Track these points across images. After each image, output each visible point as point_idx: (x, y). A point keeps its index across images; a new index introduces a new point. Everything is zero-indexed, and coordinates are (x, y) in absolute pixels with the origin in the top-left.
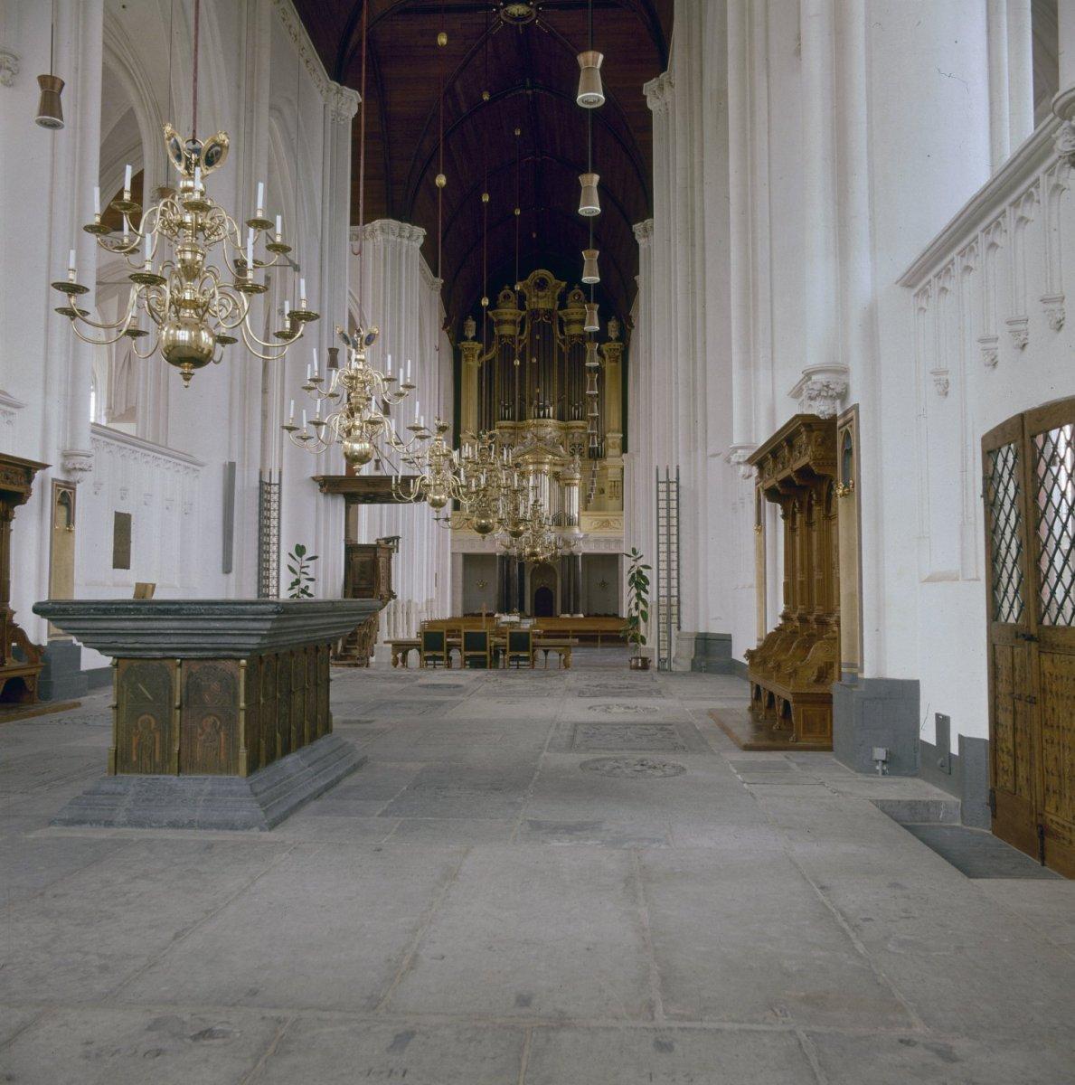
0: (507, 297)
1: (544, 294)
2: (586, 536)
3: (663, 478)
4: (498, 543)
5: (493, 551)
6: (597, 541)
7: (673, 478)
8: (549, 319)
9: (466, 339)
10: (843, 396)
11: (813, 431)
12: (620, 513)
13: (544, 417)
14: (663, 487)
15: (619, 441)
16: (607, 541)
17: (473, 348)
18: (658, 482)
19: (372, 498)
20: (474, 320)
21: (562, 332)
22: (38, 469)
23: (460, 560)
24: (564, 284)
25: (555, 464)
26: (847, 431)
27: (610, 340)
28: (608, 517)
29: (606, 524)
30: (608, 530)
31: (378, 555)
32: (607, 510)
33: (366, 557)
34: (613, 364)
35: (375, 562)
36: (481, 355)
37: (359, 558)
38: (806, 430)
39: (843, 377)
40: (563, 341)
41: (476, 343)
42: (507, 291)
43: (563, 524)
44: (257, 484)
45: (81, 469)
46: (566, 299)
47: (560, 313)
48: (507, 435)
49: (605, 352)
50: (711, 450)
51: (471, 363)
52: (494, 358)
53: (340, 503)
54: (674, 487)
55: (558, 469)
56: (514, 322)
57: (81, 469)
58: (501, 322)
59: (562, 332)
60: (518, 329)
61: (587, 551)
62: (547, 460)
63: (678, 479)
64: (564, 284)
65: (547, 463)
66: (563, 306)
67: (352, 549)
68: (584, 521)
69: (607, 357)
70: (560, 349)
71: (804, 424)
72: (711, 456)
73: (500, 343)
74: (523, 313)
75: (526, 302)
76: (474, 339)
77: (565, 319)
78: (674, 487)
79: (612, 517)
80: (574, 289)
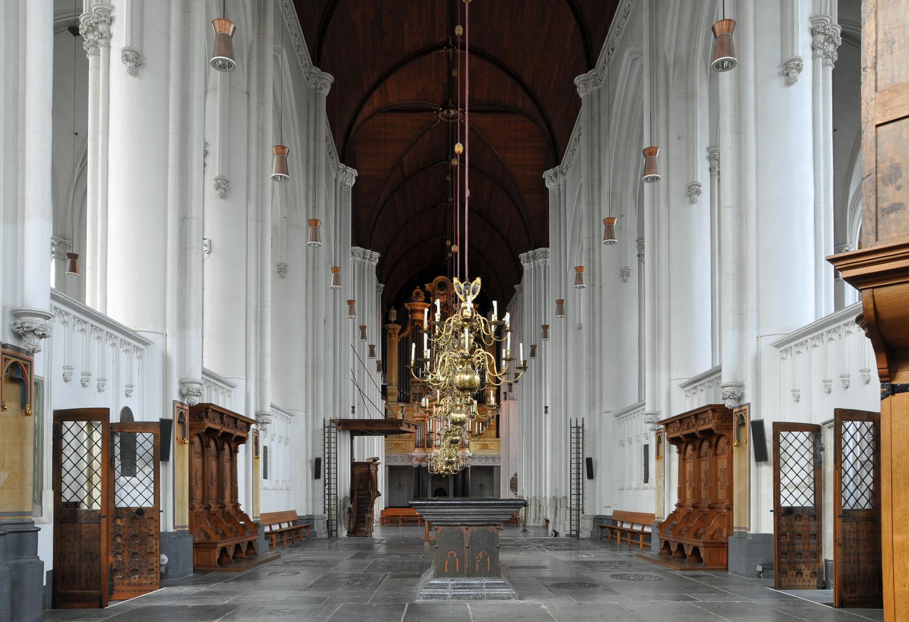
0: (418, 294)
2: (474, 455)
3: (574, 425)
5: (409, 464)
6: (480, 458)
7: (580, 424)
8: (447, 310)
9: (390, 322)
10: (739, 399)
11: (715, 412)
12: (498, 439)
14: (574, 430)
16: (487, 458)
17: (395, 329)
18: (571, 427)
19: (363, 433)
22: (252, 424)
23: (387, 468)
26: (741, 416)
28: (487, 442)
29: (485, 447)
30: (487, 450)
31: (371, 468)
32: (487, 438)
33: (364, 470)
35: (369, 472)
36: (399, 334)
37: (358, 471)
38: (712, 412)
39: (740, 389)
41: (397, 325)
42: (418, 290)
44: (323, 427)
45: (266, 423)
48: (419, 387)
50: (605, 409)
51: (393, 339)
52: (409, 335)
53: (348, 436)
54: (581, 430)
57: (266, 423)
61: (473, 464)
63: (583, 425)
67: (354, 465)
68: (472, 444)
71: (711, 409)
72: (604, 413)
76: (395, 322)
78: (581, 430)
79: (490, 442)
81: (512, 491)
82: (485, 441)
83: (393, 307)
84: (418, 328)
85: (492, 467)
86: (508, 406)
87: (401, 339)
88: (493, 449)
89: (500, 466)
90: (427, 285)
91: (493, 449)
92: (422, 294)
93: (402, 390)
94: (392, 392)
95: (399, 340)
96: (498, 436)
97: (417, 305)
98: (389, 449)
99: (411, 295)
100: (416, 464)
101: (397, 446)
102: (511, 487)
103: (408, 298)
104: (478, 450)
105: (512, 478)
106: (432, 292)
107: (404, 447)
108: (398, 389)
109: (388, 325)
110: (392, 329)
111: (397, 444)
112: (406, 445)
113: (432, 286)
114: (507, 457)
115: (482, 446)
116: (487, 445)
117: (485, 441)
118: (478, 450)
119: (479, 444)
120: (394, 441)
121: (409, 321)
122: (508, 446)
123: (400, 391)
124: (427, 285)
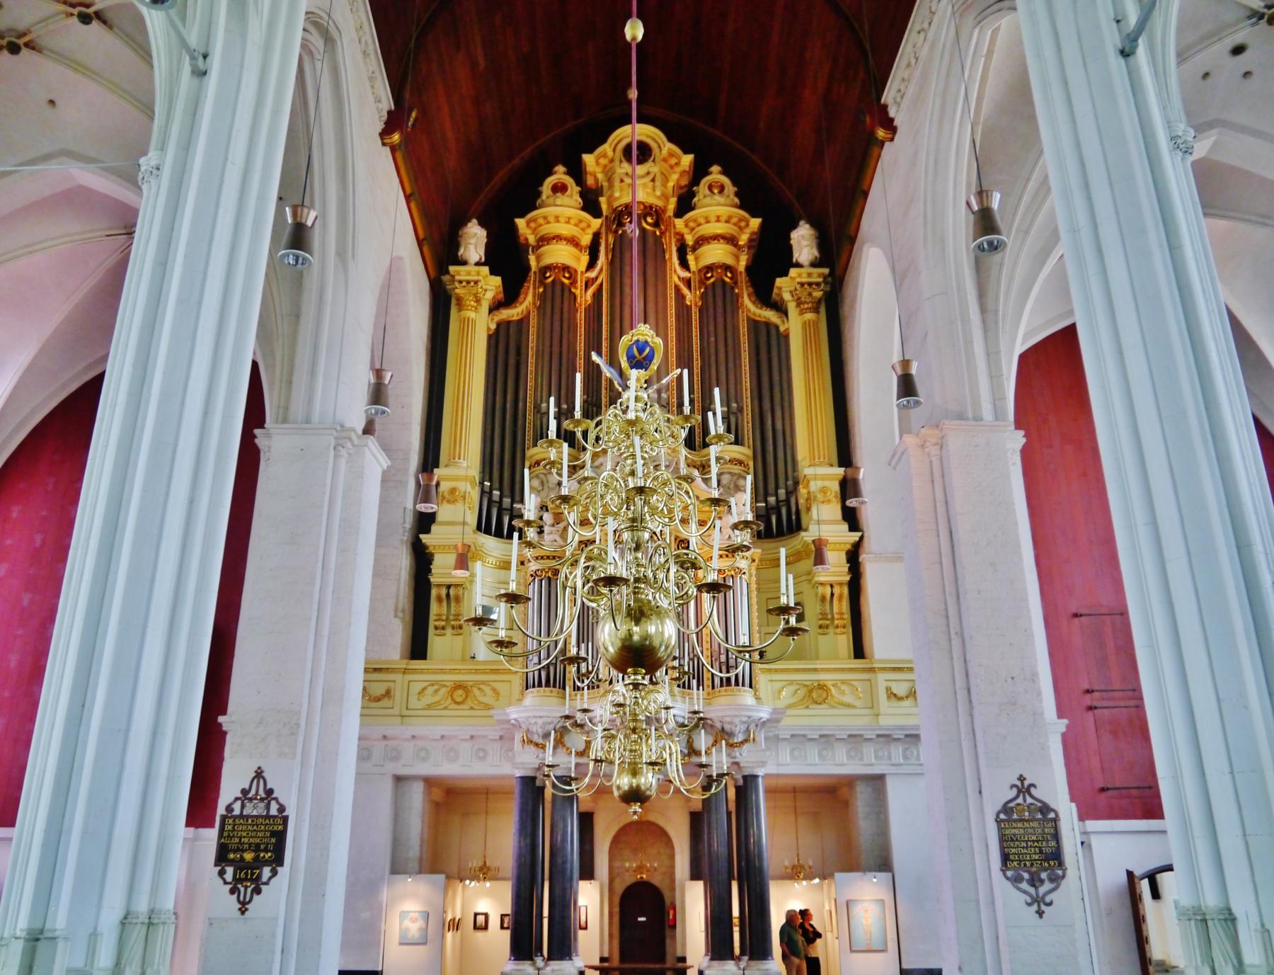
0: (560, 188)
1: (641, 170)
4: (518, 738)
6: (799, 739)
9: (464, 263)
12: (859, 663)
16: (826, 739)
17: (476, 282)
20: (482, 224)
21: (684, 264)
24: (687, 159)
27: (798, 265)
28: (822, 677)
29: (817, 694)
30: (822, 709)
32: (817, 658)
34: (810, 316)
36: (495, 307)
40: (688, 283)
42: (560, 174)
46: (693, 195)
47: (679, 223)
49: (787, 296)
56: (573, 242)
58: (544, 240)
59: (684, 264)
60: (585, 259)
64: (687, 159)
66: (685, 204)
69: (792, 308)
70: (680, 297)
73: (542, 283)
74: (596, 223)
75: (603, 200)
76: (478, 264)
77: (690, 240)
80: (708, 173)
81: (1016, 880)
82: (815, 670)
83: (475, 221)
84: (558, 288)
85: (850, 782)
86: (934, 451)
87: (499, 325)
88: (849, 706)
89: (880, 778)
90: (588, 159)
91: (849, 706)
92: (574, 189)
93: (496, 493)
94: (453, 491)
95: (493, 326)
96: (859, 651)
97: (557, 219)
98: (429, 707)
99: (539, 194)
100: (524, 761)
101: (459, 694)
102: (1005, 858)
103: (528, 201)
105: (1006, 809)
106: (605, 184)
107: (488, 699)
108: (482, 483)
109: (452, 269)
110: (468, 282)
111: (459, 686)
112: (494, 690)
113: (605, 156)
114: (962, 695)
115: (802, 693)
116: (822, 687)
117: (815, 670)
119: (791, 682)
120: (452, 671)
121: (532, 274)
122: (956, 643)
123: (490, 493)
124: (588, 159)
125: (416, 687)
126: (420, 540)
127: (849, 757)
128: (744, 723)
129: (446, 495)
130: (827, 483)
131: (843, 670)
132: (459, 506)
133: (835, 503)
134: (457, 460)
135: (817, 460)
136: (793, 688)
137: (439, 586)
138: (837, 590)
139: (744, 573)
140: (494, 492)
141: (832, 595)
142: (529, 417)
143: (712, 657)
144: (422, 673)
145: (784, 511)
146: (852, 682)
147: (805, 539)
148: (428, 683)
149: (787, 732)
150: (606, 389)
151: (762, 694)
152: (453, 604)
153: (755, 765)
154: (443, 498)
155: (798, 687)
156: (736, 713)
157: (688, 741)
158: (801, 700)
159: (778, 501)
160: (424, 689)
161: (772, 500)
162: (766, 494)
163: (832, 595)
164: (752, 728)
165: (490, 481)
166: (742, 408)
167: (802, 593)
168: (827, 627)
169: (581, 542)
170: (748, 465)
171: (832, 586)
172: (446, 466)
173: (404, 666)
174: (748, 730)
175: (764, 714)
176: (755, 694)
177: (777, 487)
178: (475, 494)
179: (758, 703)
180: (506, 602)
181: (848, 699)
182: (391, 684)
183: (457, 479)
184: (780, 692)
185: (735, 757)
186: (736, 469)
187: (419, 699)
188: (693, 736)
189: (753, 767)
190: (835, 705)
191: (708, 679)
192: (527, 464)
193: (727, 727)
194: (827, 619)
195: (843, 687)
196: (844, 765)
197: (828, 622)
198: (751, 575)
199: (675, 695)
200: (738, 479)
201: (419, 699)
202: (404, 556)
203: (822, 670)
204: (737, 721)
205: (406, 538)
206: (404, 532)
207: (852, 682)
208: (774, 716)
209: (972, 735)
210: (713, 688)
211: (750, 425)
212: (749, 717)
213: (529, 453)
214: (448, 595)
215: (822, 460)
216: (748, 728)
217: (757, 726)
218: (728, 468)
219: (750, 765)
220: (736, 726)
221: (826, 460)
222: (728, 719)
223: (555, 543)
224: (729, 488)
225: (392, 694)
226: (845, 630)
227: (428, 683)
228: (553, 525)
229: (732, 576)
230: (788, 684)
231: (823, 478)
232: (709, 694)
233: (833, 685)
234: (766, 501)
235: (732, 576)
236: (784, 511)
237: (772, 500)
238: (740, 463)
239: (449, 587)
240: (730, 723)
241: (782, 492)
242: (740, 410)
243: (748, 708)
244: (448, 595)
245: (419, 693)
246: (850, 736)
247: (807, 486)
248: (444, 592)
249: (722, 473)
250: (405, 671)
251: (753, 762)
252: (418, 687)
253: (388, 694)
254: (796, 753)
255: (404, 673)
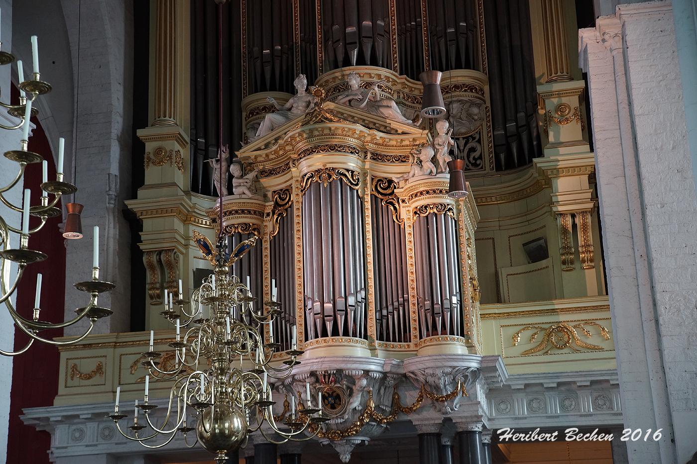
13: (361, 61)
15: (573, 102)
25: (377, 157)
28: (562, 318)
30: (564, 354)
32: (563, 297)
43: (414, 333)
55: (390, 170)
62: (353, 142)
65: (353, 151)
68: (477, 327)
88: (594, 349)
94: (158, 151)
104: (526, 353)
108: (194, 141)
115: (539, 337)
116: (561, 329)
117: (553, 311)
118: (526, 353)
119: (527, 327)
122: (642, 266)
125: (128, 361)
126: (126, 206)
127: (596, 406)
128: (447, 374)
129: (152, 156)
130: (565, 100)
131: (585, 309)
132: (166, 165)
133: (575, 121)
134: (162, 118)
135: (553, 75)
136: (529, 333)
137: (150, 253)
138: (579, 220)
139: (450, 209)
140: (210, 149)
141: (574, 226)
142: (244, 64)
143: (418, 304)
144: (133, 345)
145: (524, 137)
146: (597, 322)
147: (538, 165)
148: (138, 356)
149: (520, 382)
150: (320, 24)
151: (475, 340)
152: (167, 271)
153: (469, 420)
154: (149, 159)
155: (536, 331)
156: (439, 364)
157: (393, 398)
158: (541, 344)
159: (517, 127)
160: (136, 363)
161: (511, 125)
162: (505, 121)
163: (574, 226)
164: (460, 379)
165: (206, 137)
166: (476, 27)
167: (545, 226)
168: (572, 262)
169: (275, 192)
170: (481, 90)
171: (573, 216)
172: (152, 126)
173: (114, 340)
174: (454, 382)
175: (474, 365)
176: (467, 342)
177: (516, 112)
178: (185, 153)
179: (470, 352)
180: (13, 260)
181: (593, 341)
182: (102, 360)
183: (162, 138)
184: (514, 337)
185: (447, 413)
186: (467, 96)
187: (131, 373)
188: (400, 393)
189: (468, 423)
190: (578, 348)
191: (415, 329)
192: (244, 114)
193: (430, 379)
194: (571, 254)
195: (588, 328)
196: (591, 415)
197: (572, 257)
198: (459, 211)
199: (376, 349)
200: (470, 107)
201: (131, 373)
202: (112, 225)
203: (562, 310)
204: (439, 372)
205: (112, 206)
206: (110, 199)
207: (597, 322)
208: (485, 365)
209: (661, 374)
210: (421, 338)
211: (485, 44)
212: (454, 368)
213: (245, 101)
214: (160, 261)
215: (559, 74)
216: (454, 379)
217: (466, 377)
218: (458, 96)
219: (464, 420)
220: (439, 379)
221: (565, 73)
222: (430, 371)
223: (243, 196)
224: (460, 118)
225: (103, 370)
226: (593, 264)
227: (138, 356)
228: (241, 177)
229: (436, 215)
230: (524, 329)
231: (559, 94)
232: (416, 345)
233: (575, 327)
234: (505, 129)
235: (436, 215)
236: (524, 137)
237: (511, 125)
238: (471, 88)
239: (160, 253)
240: (433, 375)
241: (521, 115)
242: (472, 28)
243: (461, 358)
244: (160, 261)
245: (132, 367)
246: (593, 383)
247: (544, 108)
248: (154, 258)
249: (451, 102)
250: (116, 345)
251: (466, 417)
252: (134, 358)
253: (99, 369)
254: (535, 405)
255: (115, 347)
